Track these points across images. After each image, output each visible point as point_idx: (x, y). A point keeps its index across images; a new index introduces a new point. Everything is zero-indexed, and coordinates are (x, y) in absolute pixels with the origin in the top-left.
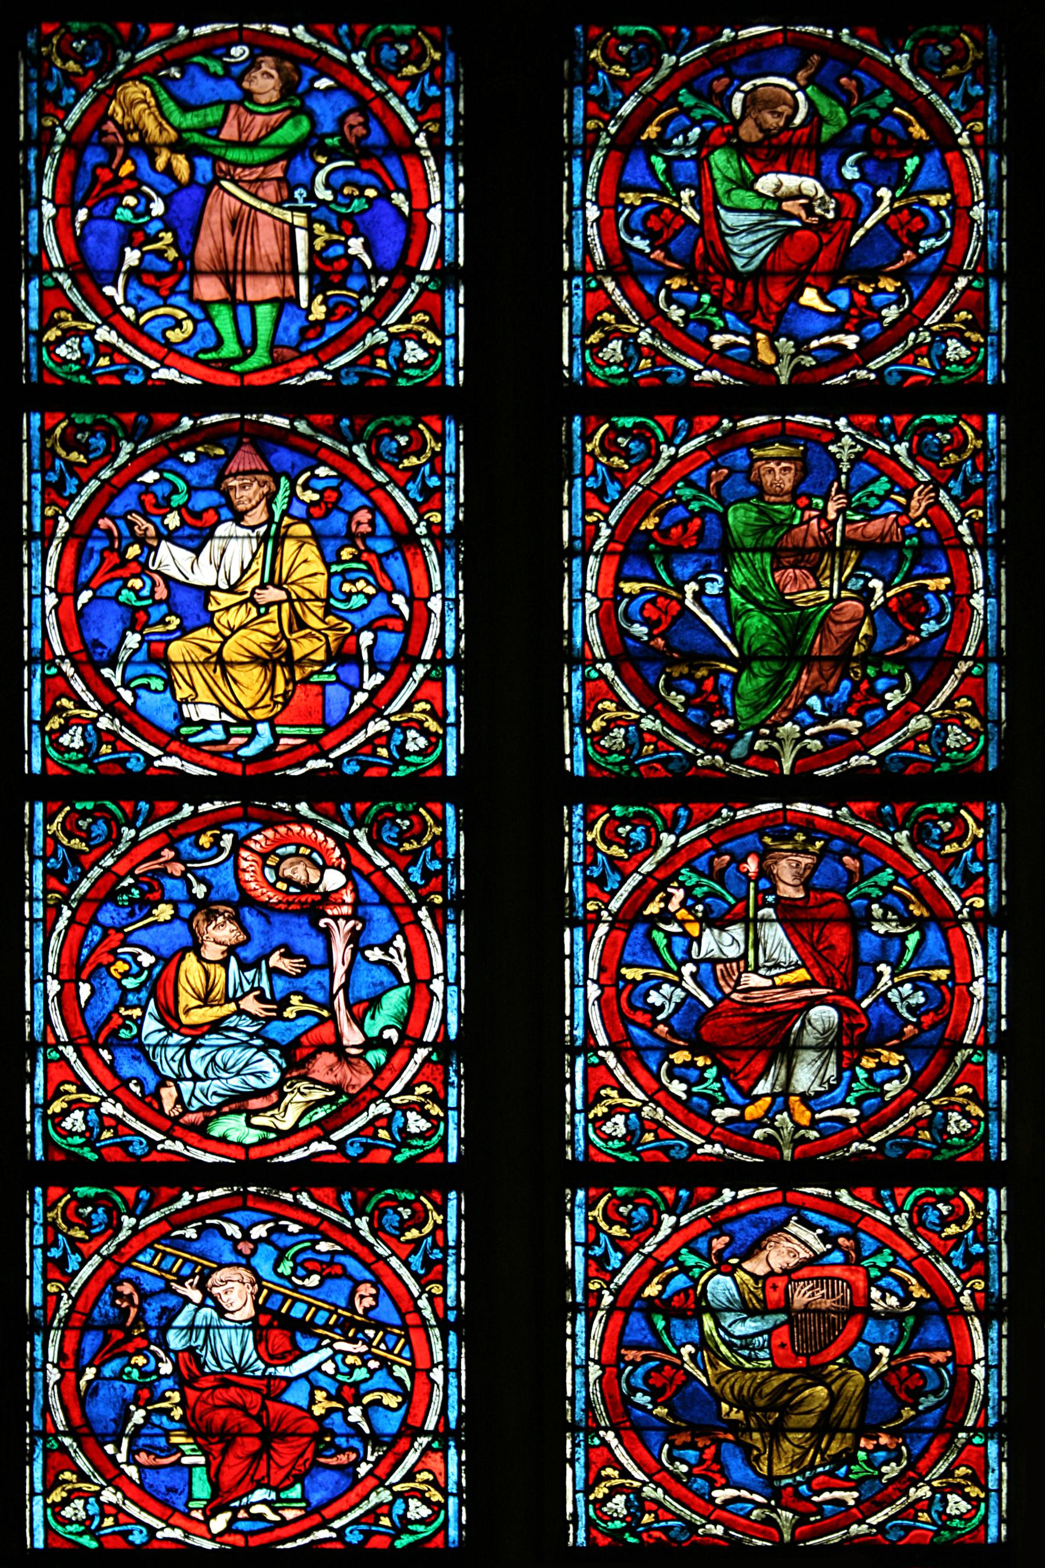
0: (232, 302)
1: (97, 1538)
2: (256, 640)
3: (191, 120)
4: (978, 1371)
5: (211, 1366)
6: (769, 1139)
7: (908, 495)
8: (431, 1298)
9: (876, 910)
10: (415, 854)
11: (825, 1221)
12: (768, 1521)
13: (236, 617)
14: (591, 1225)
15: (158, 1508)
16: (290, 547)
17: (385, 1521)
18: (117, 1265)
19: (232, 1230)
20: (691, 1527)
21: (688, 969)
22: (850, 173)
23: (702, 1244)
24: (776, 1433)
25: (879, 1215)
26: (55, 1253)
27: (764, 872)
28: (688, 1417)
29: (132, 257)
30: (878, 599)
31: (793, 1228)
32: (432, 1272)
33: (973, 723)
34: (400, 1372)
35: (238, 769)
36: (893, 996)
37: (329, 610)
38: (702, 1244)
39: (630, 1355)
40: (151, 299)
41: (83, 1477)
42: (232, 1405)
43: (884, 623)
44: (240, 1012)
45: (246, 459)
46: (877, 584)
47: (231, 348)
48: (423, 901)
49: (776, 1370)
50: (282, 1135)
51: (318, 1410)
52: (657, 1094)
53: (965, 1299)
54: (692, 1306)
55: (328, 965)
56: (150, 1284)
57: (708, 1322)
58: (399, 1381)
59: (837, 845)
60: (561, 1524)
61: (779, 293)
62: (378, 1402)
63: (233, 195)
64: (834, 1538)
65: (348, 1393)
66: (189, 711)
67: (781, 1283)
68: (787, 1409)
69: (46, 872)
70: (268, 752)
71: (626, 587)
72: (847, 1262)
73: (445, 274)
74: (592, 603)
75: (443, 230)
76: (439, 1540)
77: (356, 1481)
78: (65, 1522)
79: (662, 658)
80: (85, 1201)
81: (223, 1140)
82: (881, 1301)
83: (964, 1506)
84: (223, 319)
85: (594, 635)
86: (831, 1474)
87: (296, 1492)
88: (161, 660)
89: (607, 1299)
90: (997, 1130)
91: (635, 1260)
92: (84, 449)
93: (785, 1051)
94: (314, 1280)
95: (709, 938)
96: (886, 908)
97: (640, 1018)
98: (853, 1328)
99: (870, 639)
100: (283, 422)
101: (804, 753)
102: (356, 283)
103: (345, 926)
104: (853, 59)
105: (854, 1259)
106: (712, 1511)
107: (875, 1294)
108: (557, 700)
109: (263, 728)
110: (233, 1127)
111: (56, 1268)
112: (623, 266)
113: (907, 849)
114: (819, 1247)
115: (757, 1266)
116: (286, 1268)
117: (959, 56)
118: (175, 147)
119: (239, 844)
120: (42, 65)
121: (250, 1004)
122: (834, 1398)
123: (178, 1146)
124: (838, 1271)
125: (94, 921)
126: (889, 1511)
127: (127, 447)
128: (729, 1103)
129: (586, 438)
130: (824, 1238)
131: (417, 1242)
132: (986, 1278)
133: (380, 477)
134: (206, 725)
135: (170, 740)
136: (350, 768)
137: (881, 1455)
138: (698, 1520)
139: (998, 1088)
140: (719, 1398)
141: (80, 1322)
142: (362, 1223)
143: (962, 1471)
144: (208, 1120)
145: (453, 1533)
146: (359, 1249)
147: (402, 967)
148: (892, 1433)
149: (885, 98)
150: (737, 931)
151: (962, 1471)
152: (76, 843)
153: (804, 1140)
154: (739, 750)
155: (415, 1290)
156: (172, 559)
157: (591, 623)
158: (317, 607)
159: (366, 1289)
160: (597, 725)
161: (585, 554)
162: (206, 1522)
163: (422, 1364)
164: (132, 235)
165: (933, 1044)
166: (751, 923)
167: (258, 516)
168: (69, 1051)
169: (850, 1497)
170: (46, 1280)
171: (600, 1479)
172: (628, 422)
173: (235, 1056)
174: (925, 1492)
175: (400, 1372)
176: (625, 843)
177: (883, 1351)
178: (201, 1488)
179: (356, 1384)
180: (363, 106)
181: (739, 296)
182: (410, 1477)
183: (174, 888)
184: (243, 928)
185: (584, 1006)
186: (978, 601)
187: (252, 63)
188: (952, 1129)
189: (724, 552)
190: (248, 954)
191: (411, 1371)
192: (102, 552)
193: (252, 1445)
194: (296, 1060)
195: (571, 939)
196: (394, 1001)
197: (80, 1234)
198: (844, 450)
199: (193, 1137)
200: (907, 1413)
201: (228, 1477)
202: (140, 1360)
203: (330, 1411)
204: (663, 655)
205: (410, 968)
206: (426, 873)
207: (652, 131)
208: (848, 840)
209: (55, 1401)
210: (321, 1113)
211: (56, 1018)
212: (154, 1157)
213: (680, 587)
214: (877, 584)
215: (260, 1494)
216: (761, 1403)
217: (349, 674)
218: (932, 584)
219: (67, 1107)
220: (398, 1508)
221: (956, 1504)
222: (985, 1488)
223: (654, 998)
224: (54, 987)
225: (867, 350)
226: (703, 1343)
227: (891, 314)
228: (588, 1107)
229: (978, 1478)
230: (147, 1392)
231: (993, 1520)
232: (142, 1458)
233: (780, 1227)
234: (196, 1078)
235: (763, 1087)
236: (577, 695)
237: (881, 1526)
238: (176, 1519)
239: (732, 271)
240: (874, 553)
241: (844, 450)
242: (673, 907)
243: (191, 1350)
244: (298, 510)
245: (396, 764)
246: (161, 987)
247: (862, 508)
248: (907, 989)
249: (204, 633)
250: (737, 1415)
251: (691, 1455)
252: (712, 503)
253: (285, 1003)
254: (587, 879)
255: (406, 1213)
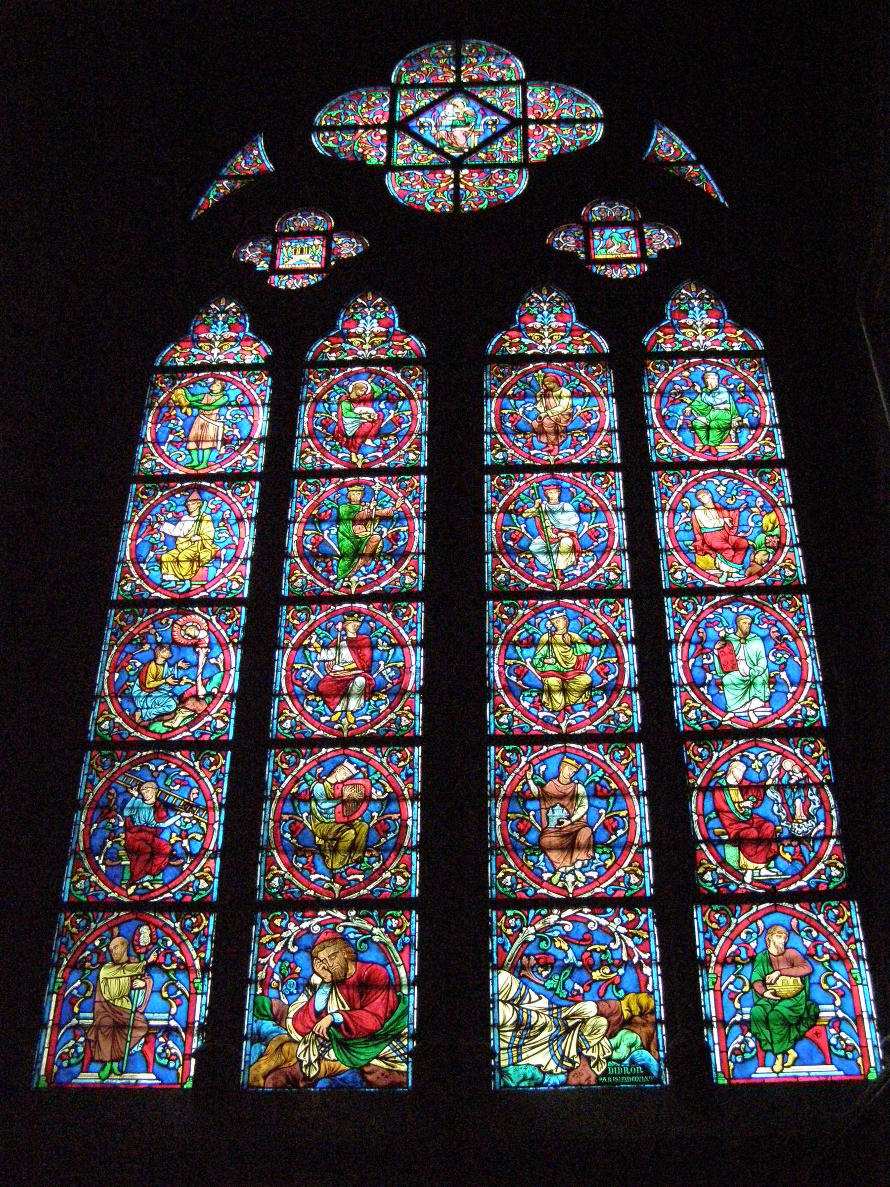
0: (197, 449)
1: (87, 897)
2: (189, 553)
3: (194, 398)
4: (409, 822)
5: (137, 823)
6: (340, 729)
7: (396, 500)
8: (218, 794)
9: (380, 641)
10: (230, 624)
11: (358, 761)
12: (331, 889)
13: (184, 546)
14: (275, 763)
15: (109, 883)
16: (204, 523)
17: (191, 889)
18: (111, 781)
19: (152, 767)
20: (301, 891)
21: (316, 664)
22: (382, 406)
23: (313, 771)
24: (335, 850)
25: (376, 758)
26: (91, 777)
27: (344, 629)
28: (304, 849)
29: (171, 437)
30: (385, 535)
31: (346, 763)
32: (218, 783)
33: (414, 575)
34: (203, 825)
35: (177, 596)
36: (384, 673)
37: (213, 542)
38: (313, 771)
39: (286, 817)
40: (174, 449)
41: (86, 870)
42: (142, 839)
43: (387, 542)
44: (166, 683)
45: (195, 495)
46: (385, 529)
47: (195, 463)
48: (231, 641)
49: (337, 823)
50: (174, 729)
51: (172, 841)
52: (302, 712)
53: (406, 792)
54: (309, 797)
55: (197, 665)
56: (121, 789)
57: (313, 804)
58: (202, 828)
59: (368, 618)
60: (254, 890)
61: (359, 441)
62: (193, 838)
63: (200, 421)
64: (354, 896)
65: (184, 833)
66: (165, 577)
67: (340, 786)
68: (339, 840)
69: (112, 634)
70: (189, 590)
71: (306, 532)
72: (364, 778)
73: (261, 440)
74: (295, 538)
75: (262, 427)
76: (209, 898)
77: (182, 872)
78: (77, 889)
79: (315, 556)
80: (104, 756)
81: (154, 732)
82: (377, 794)
83: (403, 881)
84: (194, 453)
85: (295, 548)
86: (354, 867)
87: (160, 877)
88: (159, 561)
89: (279, 794)
90: (419, 723)
91: (290, 777)
92: (147, 494)
93: (346, 694)
94: (178, 787)
95: (324, 652)
96: (383, 640)
97: (299, 683)
98: (364, 806)
99: (382, 548)
100: (207, 484)
101: (359, 586)
102: (235, 442)
103: (205, 651)
104: (384, 376)
105: (366, 777)
106: (310, 884)
107: (373, 790)
108: (281, 570)
109: (188, 582)
110: (158, 727)
111: (90, 783)
112: (312, 435)
113: (391, 619)
114: (355, 771)
115: (332, 780)
116: (168, 782)
117: (415, 374)
118: (189, 406)
119: (174, 622)
120: (154, 386)
121: (170, 680)
122: (357, 834)
123: (139, 734)
124: (360, 781)
125: (123, 651)
126: (375, 884)
127: (160, 493)
128: (326, 715)
129: (298, 486)
130: (357, 768)
131: (215, 771)
132: (413, 783)
133: (234, 500)
134: (170, 581)
135: (158, 587)
136: (213, 595)
137: (373, 859)
138: (304, 888)
139: (419, 708)
140: (315, 835)
141: (96, 805)
142: (197, 764)
143: (402, 866)
144: (150, 724)
145: (215, 894)
146: (195, 775)
147: (221, 665)
148: (377, 849)
149: (393, 385)
150: (333, 650)
151: (402, 866)
152: (123, 623)
153: (351, 729)
154: (338, 586)
155: (212, 790)
156: (167, 528)
157: (294, 544)
158: (210, 542)
159: (195, 791)
160: (293, 578)
161: (295, 522)
162: (126, 890)
163: (211, 821)
164: (172, 431)
165: (399, 693)
166: (338, 648)
167: (196, 513)
168: (108, 699)
169: (361, 877)
170: (86, 788)
171: (270, 870)
172: (311, 481)
173: (161, 700)
174: (388, 875)
175: (203, 825)
176: (299, 619)
177: (375, 814)
178: (127, 876)
179: (186, 831)
180: (243, 393)
181: (347, 442)
182: (202, 870)
183: (151, 638)
184: (171, 652)
185: (280, 679)
186: (416, 534)
187: (214, 382)
188: (403, 724)
189: (339, 520)
190: (172, 662)
191: (207, 824)
192: (147, 525)
193: (148, 857)
194: (182, 700)
195: (278, 654)
196: (217, 678)
197: (100, 769)
198: (376, 488)
199: (143, 731)
200: (383, 840)
201: (137, 870)
202: (113, 821)
203: (177, 841)
204: (317, 556)
205: (224, 666)
206: (234, 632)
207: (325, 397)
208: (372, 617)
209: (81, 838)
210: (188, 720)
211: (106, 686)
212: (130, 739)
213: (323, 532)
214: (385, 529)
215: (148, 878)
216: (330, 837)
217: (217, 564)
218: (402, 529)
219: (105, 719)
220: (196, 884)
221: (400, 880)
222: (410, 873)
223: (304, 675)
224: (107, 674)
225: (386, 457)
226: (311, 812)
227: (392, 446)
228: (279, 716)
229: (408, 869)
230: (113, 834)
231: (413, 888)
232: (108, 862)
233: (340, 764)
234: (148, 708)
235: (338, 708)
236: (288, 568)
237: (371, 891)
238: (116, 889)
239: (345, 435)
240: (384, 519)
241: (376, 488)
242: (313, 641)
243: (131, 816)
244: (208, 511)
245: (228, 593)
246: (141, 674)
247: (381, 505)
248: (389, 670)
249: (175, 551)
250: (321, 842)
251: (304, 860)
252: (335, 505)
253: (181, 679)
254: (286, 632)
255: (212, 759)
